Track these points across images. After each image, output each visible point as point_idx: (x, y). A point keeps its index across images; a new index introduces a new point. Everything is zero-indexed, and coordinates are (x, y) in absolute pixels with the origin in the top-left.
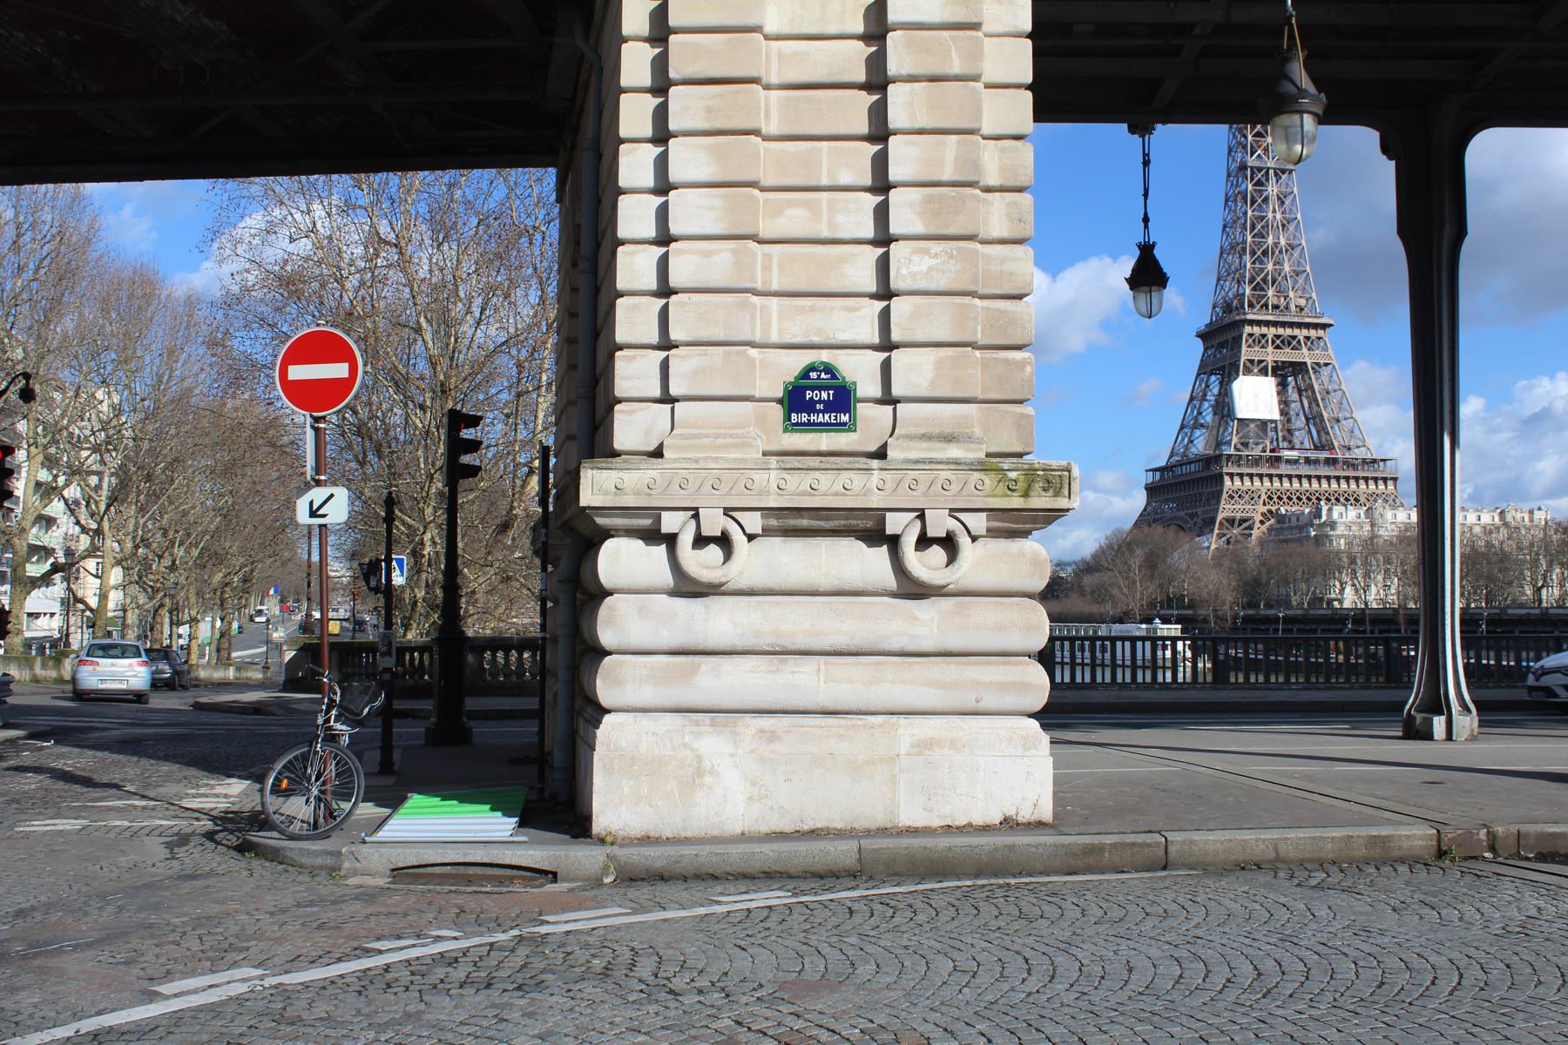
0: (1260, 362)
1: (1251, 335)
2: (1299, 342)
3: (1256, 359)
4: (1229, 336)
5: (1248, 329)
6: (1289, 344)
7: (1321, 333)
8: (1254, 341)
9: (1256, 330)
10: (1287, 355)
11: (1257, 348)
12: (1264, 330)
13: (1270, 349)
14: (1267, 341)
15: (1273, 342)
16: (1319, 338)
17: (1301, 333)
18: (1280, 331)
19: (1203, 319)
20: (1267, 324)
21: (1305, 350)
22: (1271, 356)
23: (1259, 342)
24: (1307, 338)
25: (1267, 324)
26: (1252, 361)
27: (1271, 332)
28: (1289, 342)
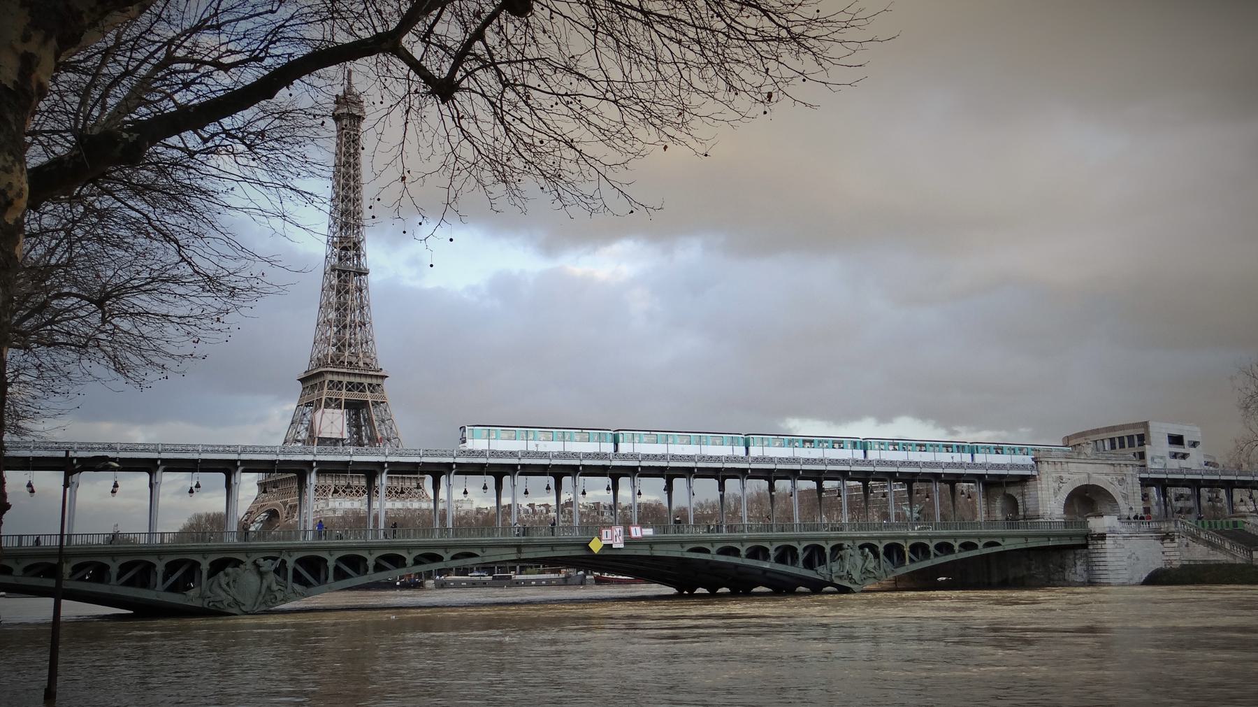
0: (336, 400)
1: (331, 381)
2: (364, 387)
3: (334, 397)
4: (317, 381)
5: (330, 377)
6: (358, 388)
7: (379, 381)
8: (333, 385)
9: (336, 378)
10: (355, 396)
11: (335, 390)
12: (341, 378)
13: (344, 391)
14: (342, 386)
15: (347, 386)
16: (379, 385)
17: (366, 381)
18: (352, 379)
19: (302, 367)
20: (343, 374)
21: (368, 393)
22: (344, 395)
23: (337, 386)
24: (370, 385)
25: (343, 374)
26: (331, 399)
27: (346, 379)
28: (359, 387)
